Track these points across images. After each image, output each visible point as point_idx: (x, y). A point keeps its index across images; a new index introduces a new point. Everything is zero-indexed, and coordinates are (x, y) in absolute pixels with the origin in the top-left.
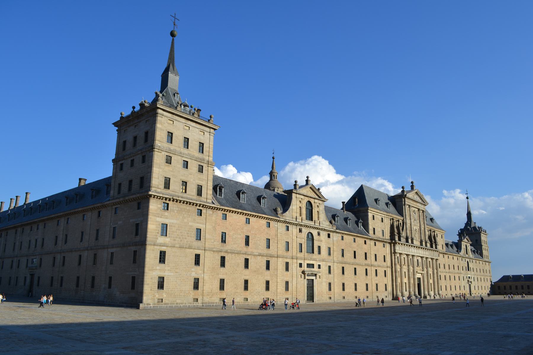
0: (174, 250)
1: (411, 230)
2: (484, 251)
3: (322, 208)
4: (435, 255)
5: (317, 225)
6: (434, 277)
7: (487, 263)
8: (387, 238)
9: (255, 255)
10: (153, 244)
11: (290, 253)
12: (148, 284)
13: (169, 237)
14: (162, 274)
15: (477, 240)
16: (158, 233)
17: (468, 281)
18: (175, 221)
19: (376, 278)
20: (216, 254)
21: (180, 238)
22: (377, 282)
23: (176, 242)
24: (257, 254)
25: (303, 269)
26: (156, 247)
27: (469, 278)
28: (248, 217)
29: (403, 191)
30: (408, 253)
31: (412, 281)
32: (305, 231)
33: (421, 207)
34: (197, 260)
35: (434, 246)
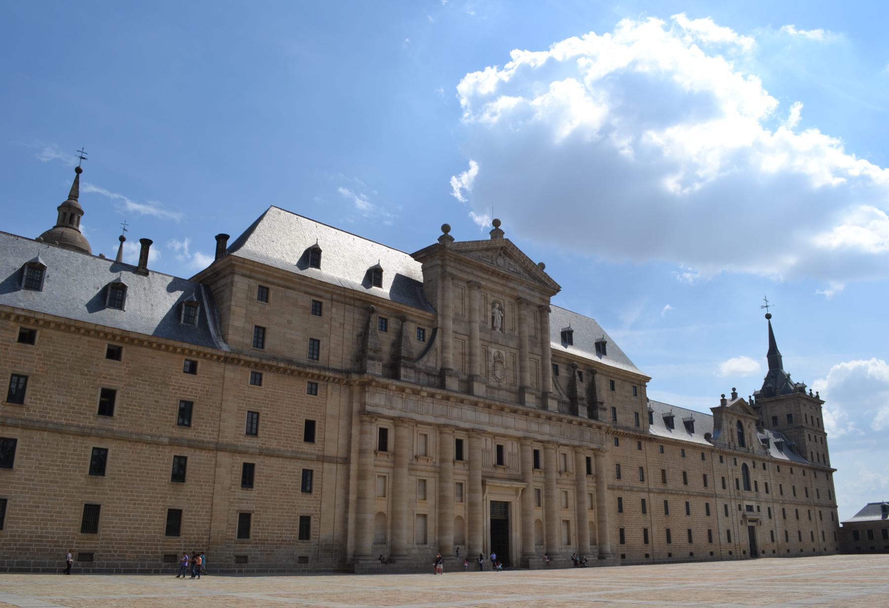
1: (471, 354)
2: (807, 443)
4: (591, 438)
6: (580, 503)
7: (821, 475)
8: (336, 365)
15: (789, 416)
17: (744, 516)
19: (241, 493)
22: (245, 507)
27: (750, 508)
29: (446, 238)
30: (442, 421)
31: (457, 509)
33: (536, 298)
35: (583, 411)
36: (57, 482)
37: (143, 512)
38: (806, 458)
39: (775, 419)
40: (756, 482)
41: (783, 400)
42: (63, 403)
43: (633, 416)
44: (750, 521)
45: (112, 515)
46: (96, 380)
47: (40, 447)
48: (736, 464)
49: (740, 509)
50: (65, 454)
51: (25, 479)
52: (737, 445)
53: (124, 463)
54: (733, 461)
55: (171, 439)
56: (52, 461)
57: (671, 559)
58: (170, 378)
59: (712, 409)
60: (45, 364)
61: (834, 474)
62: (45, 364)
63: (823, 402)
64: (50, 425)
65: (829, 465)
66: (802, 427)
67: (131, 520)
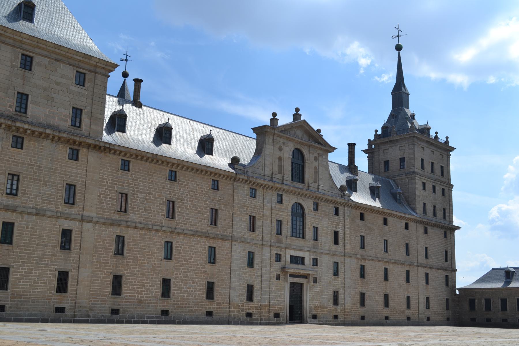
15: (402, 160)
17: (283, 269)
38: (414, 210)
39: (387, 163)
40: (316, 229)
41: (397, 141)
43: (68, 113)
44: (292, 276)
48: (280, 202)
49: (278, 258)
52: (288, 176)
54: (275, 198)
57: (115, 317)
59: (255, 130)
61: (457, 232)
63: (452, 149)
65: (451, 221)
66: (414, 173)
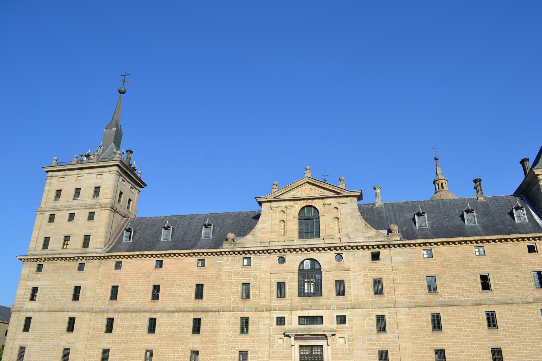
0: (42, 314)
3: (349, 208)
5: (329, 243)
9: (168, 312)
10: (17, 310)
11: (251, 302)
12: (6, 355)
13: (38, 301)
14: (23, 344)
16: (26, 298)
18: (47, 283)
20: (100, 316)
21: (51, 301)
23: (46, 305)
24: (174, 309)
25: (287, 326)
26: (21, 314)
28: (161, 259)
32: (294, 261)
34: (71, 325)
36: (470, 336)
37: (531, 350)
42: (459, 288)
45: (511, 353)
46: (474, 270)
47: (454, 316)
50: (470, 318)
51: (451, 336)
53: (508, 319)
55: (534, 299)
56: (463, 324)
58: (521, 259)
60: (443, 267)
62: (443, 267)
64: (456, 303)
67: (524, 356)
